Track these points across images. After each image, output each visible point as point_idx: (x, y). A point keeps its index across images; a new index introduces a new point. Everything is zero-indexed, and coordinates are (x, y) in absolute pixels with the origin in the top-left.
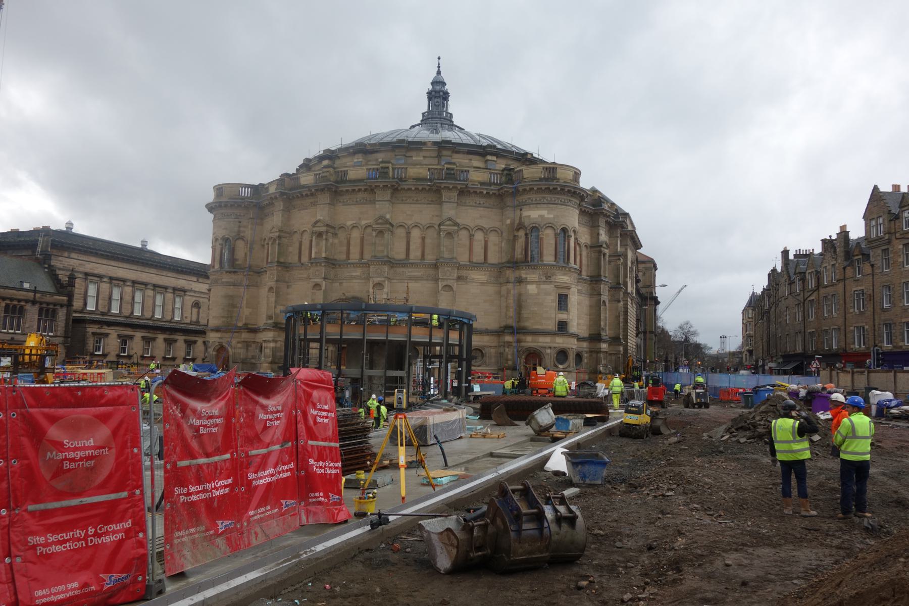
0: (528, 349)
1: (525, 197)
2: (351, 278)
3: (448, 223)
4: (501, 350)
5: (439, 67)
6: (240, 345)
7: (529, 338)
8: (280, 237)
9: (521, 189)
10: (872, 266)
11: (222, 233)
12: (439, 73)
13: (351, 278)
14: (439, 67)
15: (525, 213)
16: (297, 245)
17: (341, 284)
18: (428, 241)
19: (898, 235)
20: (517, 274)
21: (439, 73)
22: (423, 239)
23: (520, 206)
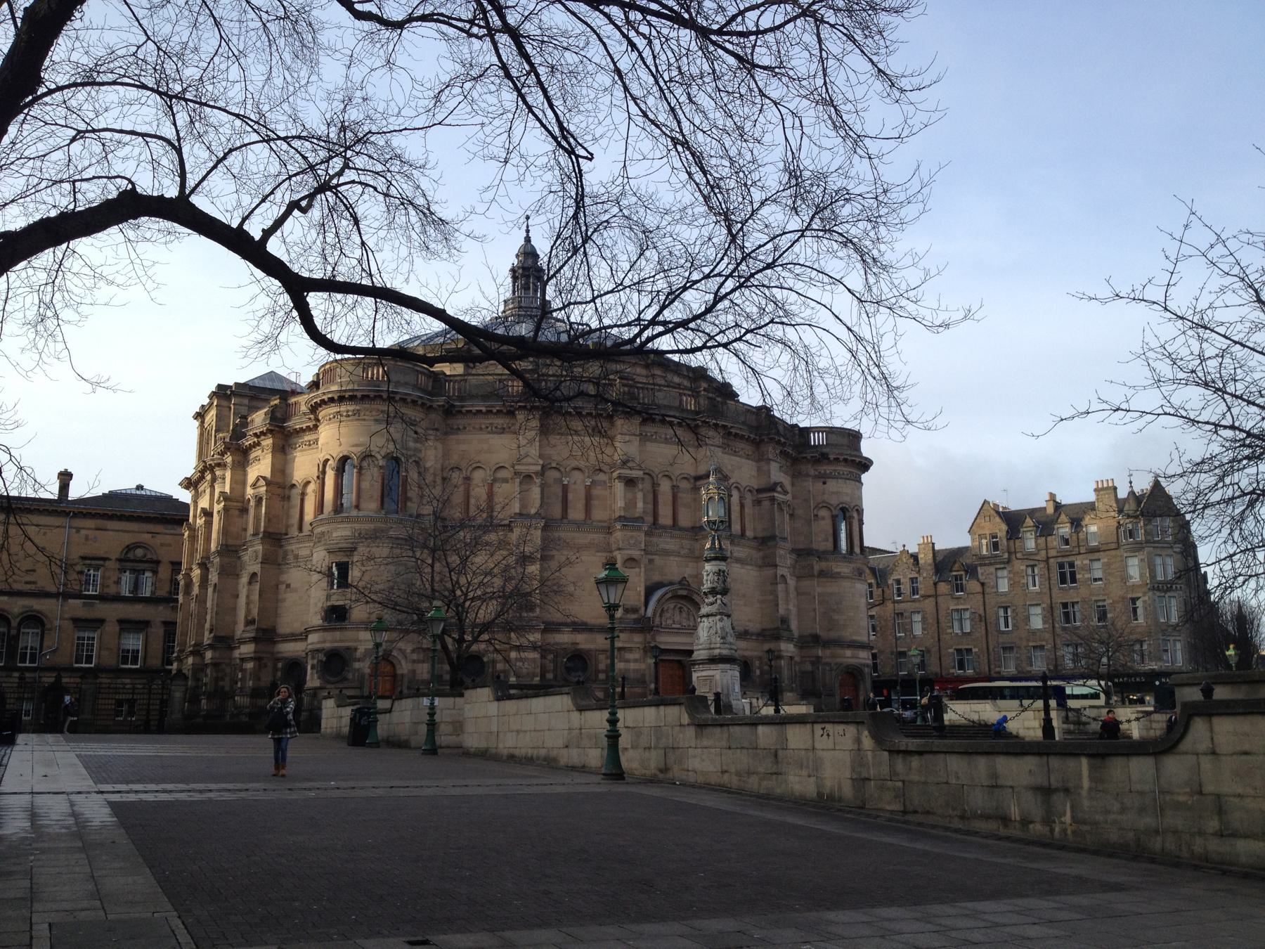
0: (848, 666)
1: (827, 469)
2: (666, 553)
3: (779, 489)
4: (809, 667)
5: (528, 231)
6: (415, 656)
7: (848, 653)
8: (542, 474)
9: (832, 457)
10: (983, 584)
11: (380, 445)
12: (528, 239)
13: (666, 553)
14: (528, 231)
15: (832, 485)
16: (559, 491)
17: (651, 561)
18: (747, 510)
19: (1019, 555)
20: (824, 565)
21: (528, 239)
22: (742, 506)
23: (824, 478)
